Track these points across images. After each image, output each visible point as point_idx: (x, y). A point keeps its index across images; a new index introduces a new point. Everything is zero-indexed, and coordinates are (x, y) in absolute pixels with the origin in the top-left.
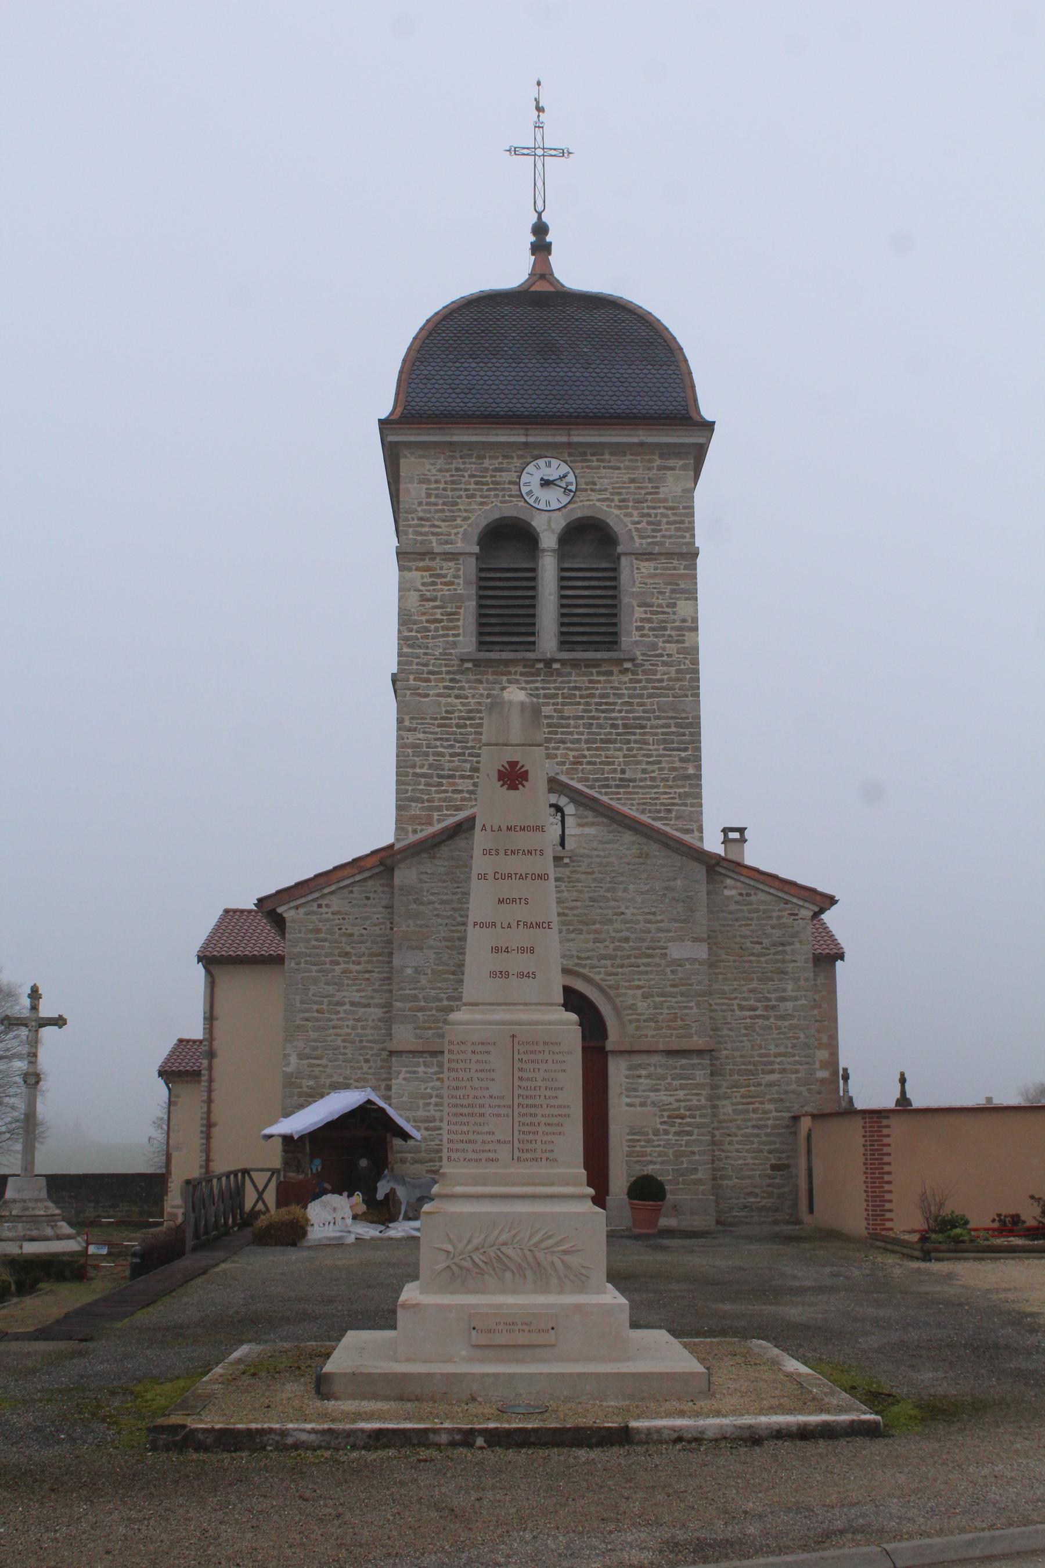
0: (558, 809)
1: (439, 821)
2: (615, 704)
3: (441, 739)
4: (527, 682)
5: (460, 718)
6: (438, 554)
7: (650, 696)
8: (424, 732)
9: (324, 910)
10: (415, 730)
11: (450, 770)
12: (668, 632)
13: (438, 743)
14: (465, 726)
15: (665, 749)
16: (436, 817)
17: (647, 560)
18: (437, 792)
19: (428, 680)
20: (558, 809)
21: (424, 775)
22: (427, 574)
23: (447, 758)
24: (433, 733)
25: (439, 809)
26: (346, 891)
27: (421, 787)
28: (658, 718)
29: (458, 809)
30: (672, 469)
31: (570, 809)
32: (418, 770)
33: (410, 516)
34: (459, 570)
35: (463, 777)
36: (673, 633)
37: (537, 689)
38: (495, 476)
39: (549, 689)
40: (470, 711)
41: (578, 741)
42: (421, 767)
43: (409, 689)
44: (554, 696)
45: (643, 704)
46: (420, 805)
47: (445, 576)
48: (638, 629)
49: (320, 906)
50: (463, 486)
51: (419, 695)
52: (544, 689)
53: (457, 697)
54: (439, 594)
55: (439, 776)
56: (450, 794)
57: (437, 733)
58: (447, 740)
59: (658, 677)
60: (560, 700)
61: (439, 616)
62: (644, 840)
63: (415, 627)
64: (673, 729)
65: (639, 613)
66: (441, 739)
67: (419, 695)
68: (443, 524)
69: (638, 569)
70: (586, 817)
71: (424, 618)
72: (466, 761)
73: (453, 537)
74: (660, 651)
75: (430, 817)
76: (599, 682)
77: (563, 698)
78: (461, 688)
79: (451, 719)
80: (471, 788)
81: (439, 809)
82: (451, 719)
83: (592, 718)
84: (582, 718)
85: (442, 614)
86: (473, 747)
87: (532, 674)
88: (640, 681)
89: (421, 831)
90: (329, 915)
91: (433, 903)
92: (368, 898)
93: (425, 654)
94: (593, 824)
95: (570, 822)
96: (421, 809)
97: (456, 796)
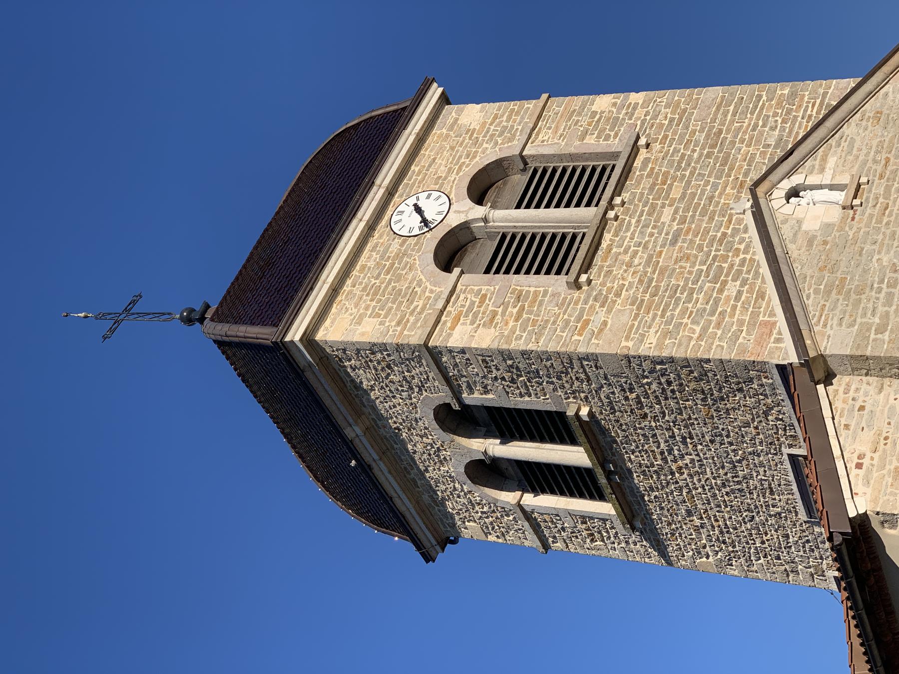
0: (794, 193)
1: (772, 314)
2: (683, 155)
3: (664, 311)
4: (627, 230)
5: (645, 292)
6: (445, 307)
7: (687, 128)
8: (650, 327)
9: (866, 462)
10: (643, 336)
11: (707, 303)
12: (621, 116)
13: (668, 314)
14: (657, 288)
15: (752, 113)
16: (766, 318)
17: (538, 134)
18: (732, 315)
19: (587, 322)
20: (794, 193)
21: (705, 329)
22: (462, 319)
23: (690, 305)
24: (654, 319)
25: (755, 315)
26: (843, 434)
27: (719, 332)
28: (714, 120)
29: (761, 295)
30: (457, 120)
31: (797, 179)
32: (696, 336)
33: (390, 333)
34: (473, 290)
35: (721, 291)
36: (624, 111)
37: (638, 221)
38: (389, 257)
39: (643, 211)
40: (641, 281)
41: (715, 186)
42: (694, 331)
43: (590, 339)
44: (653, 207)
45: (694, 132)
46: (744, 334)
47: (473, 303)
48: (607, 138)
49: (859, 466)
50: (383, 286)
51: (601, 330)
52: (641, 215)
53: (618, 295)
54: (490, 308)
55: (712, 313)
56: (739, 304)
57: (655, 316)
58: (667, 305)
59: (667, 122)
60: (659, 202)
61: (515, 310)
62: (858, 115)
63: (518, 333)
64: (732, 108)
65: (590, 140)
66: (664, 311)
67: (601, 330)
68: (415, 303)
69: (543, 141)
70: (813, 166)
71: (511, 324)
72: (701, 288)
73: (433, 296)
74: (639, 123)
75: (765, 324)
76: (652, 169)
77: (658, 199)
78: (609, 290)
79: (642, 301)
80: (738, 283)
81: (755, 315)
82: (642, 301)
83: (692, 173)
84: (689, 182)
85: (515, 307)
86: (687, 280)
87: (621, 225)
88: (665, 137)
89: (780, 333)
90: (876, 456)
91: (887, 313)
92: (862, 408)
93: (554, 322)
94: (824, 160)
95: (812, 180)
96: (748, 333)
97: (743, 298)
